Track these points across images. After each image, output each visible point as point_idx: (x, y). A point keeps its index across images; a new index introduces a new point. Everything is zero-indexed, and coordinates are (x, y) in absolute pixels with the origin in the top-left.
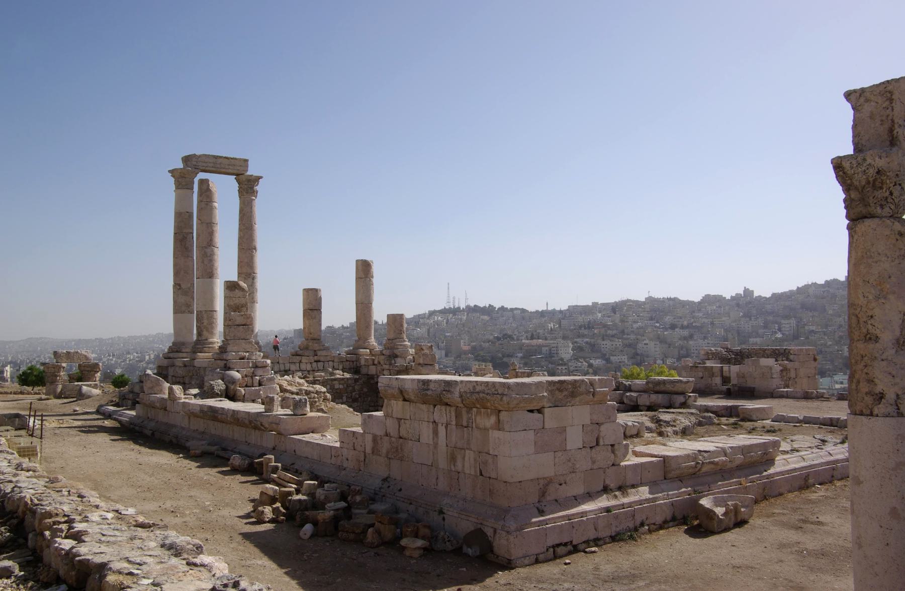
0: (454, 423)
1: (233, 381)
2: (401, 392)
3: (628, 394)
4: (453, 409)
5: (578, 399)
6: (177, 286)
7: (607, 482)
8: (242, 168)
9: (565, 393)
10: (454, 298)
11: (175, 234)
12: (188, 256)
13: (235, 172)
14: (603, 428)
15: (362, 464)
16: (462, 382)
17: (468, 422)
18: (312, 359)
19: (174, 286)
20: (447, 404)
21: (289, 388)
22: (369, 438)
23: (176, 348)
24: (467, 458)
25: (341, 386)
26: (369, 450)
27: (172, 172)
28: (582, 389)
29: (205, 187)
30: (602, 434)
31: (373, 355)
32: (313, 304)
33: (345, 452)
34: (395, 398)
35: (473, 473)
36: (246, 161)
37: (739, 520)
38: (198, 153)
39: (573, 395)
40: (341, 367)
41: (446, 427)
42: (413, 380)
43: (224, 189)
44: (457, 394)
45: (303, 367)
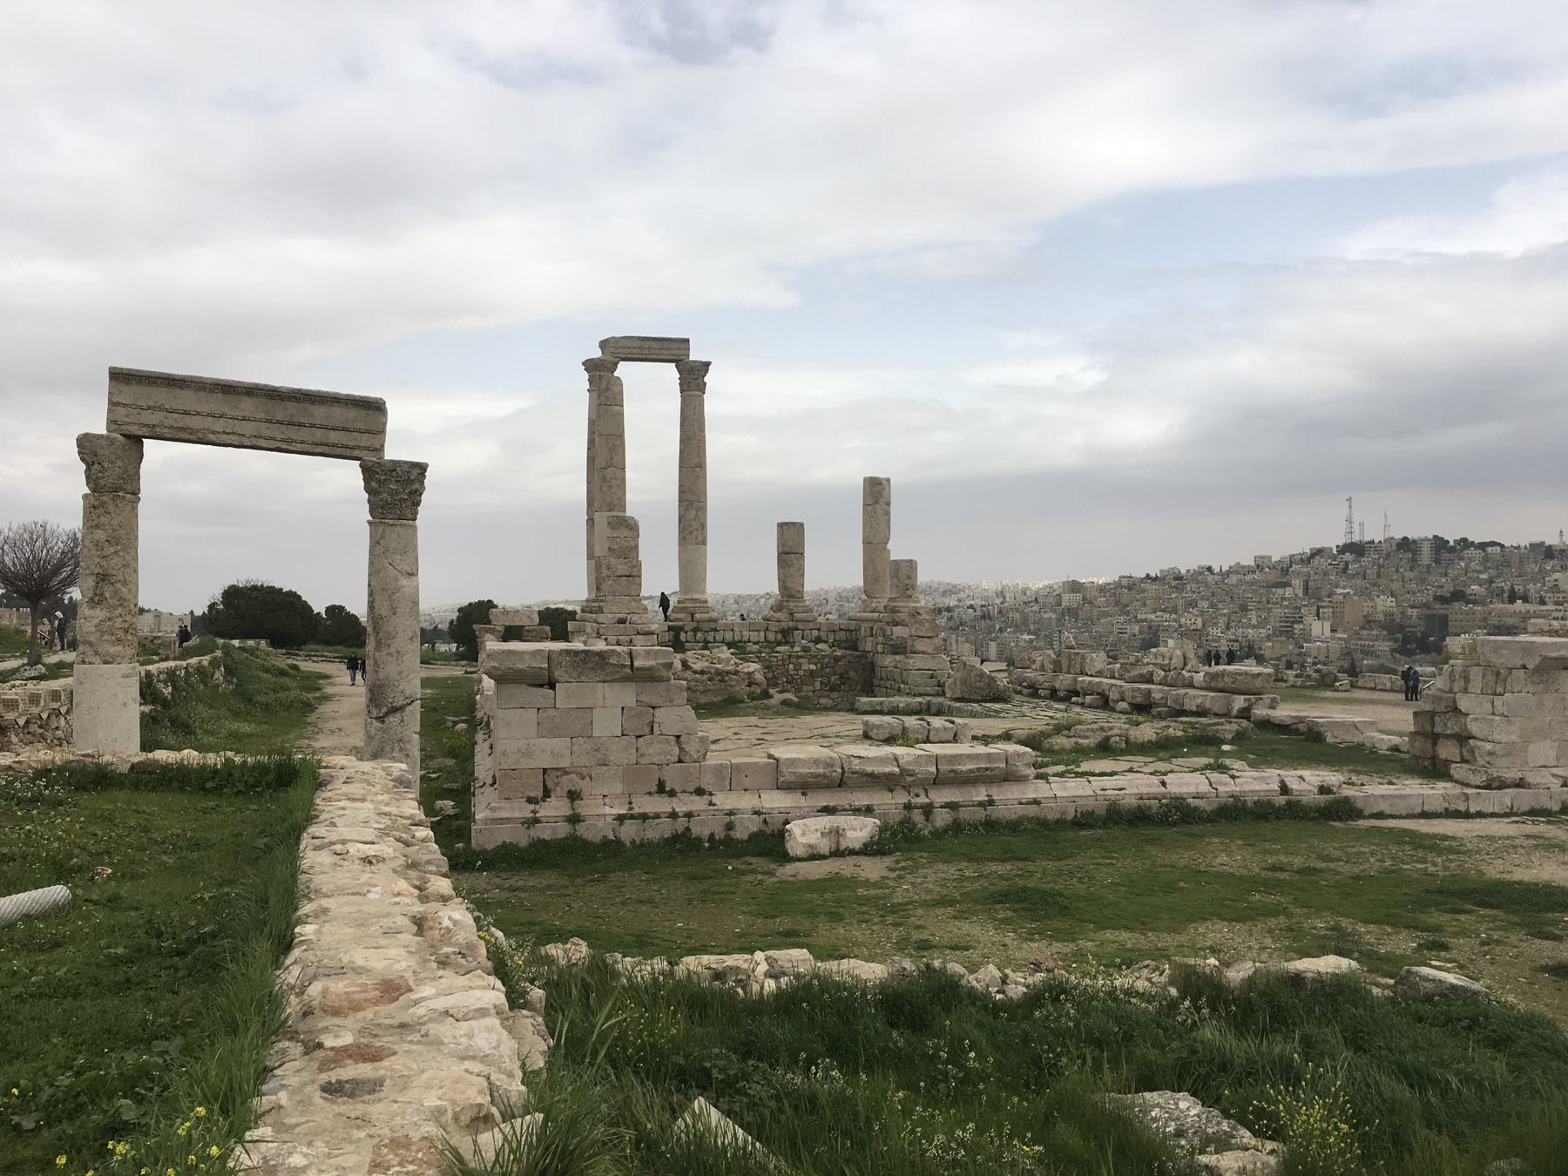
10: (1361, 525)
14: (658, 712)
25: (813, 667)
32: (791, 545)
36: (687, 341)
37: (843, 847)
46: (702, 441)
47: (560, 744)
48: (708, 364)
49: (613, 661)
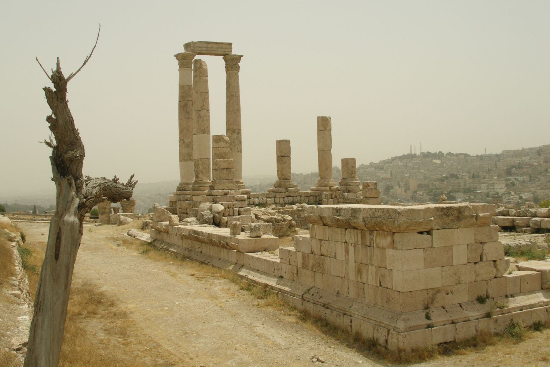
0: (360, 243)
1: (218, 213)
2: (321, 218)
3: (534, 219)
4: (359, 231)
5: (463, 222)
6: (182, 140)
7: (490, 292)
8: (227, 50)
9: (452, 217)
11: (180, 101)
12: (189, 118)
13: (222, 53)
14: (486, 247)
15: (295, 276)
16: (364, 209)
17: (370, 242)
18: (284, 195)
19: (180, 141)
20: (355, 228)
21: (262, 217)
22: (300, 255)
23: (182, 188)
24: (369, 272)
26: (299, 265)
27: (178, 56)
28: (467, 213)
29: (198, 65)
30: (485, 251)
31: (332, 191)
33: (284, 266)
34: (318, 224)
35: (374, 284)
36: (230, 44)
38: (195, 40)
39: (458, 219)
40: (307, 201)
41: (355, 247)
42: (328, 208)
43: (215, 66)
44: (360, 220)
45: (277, 200)
46: (238, 97)
47: (436, 271)
48: (241, 56)
49: (467, 213)
